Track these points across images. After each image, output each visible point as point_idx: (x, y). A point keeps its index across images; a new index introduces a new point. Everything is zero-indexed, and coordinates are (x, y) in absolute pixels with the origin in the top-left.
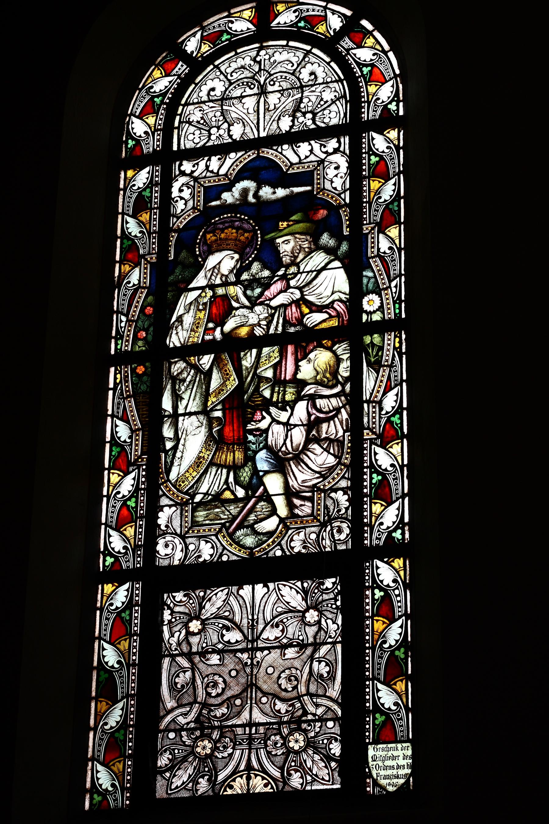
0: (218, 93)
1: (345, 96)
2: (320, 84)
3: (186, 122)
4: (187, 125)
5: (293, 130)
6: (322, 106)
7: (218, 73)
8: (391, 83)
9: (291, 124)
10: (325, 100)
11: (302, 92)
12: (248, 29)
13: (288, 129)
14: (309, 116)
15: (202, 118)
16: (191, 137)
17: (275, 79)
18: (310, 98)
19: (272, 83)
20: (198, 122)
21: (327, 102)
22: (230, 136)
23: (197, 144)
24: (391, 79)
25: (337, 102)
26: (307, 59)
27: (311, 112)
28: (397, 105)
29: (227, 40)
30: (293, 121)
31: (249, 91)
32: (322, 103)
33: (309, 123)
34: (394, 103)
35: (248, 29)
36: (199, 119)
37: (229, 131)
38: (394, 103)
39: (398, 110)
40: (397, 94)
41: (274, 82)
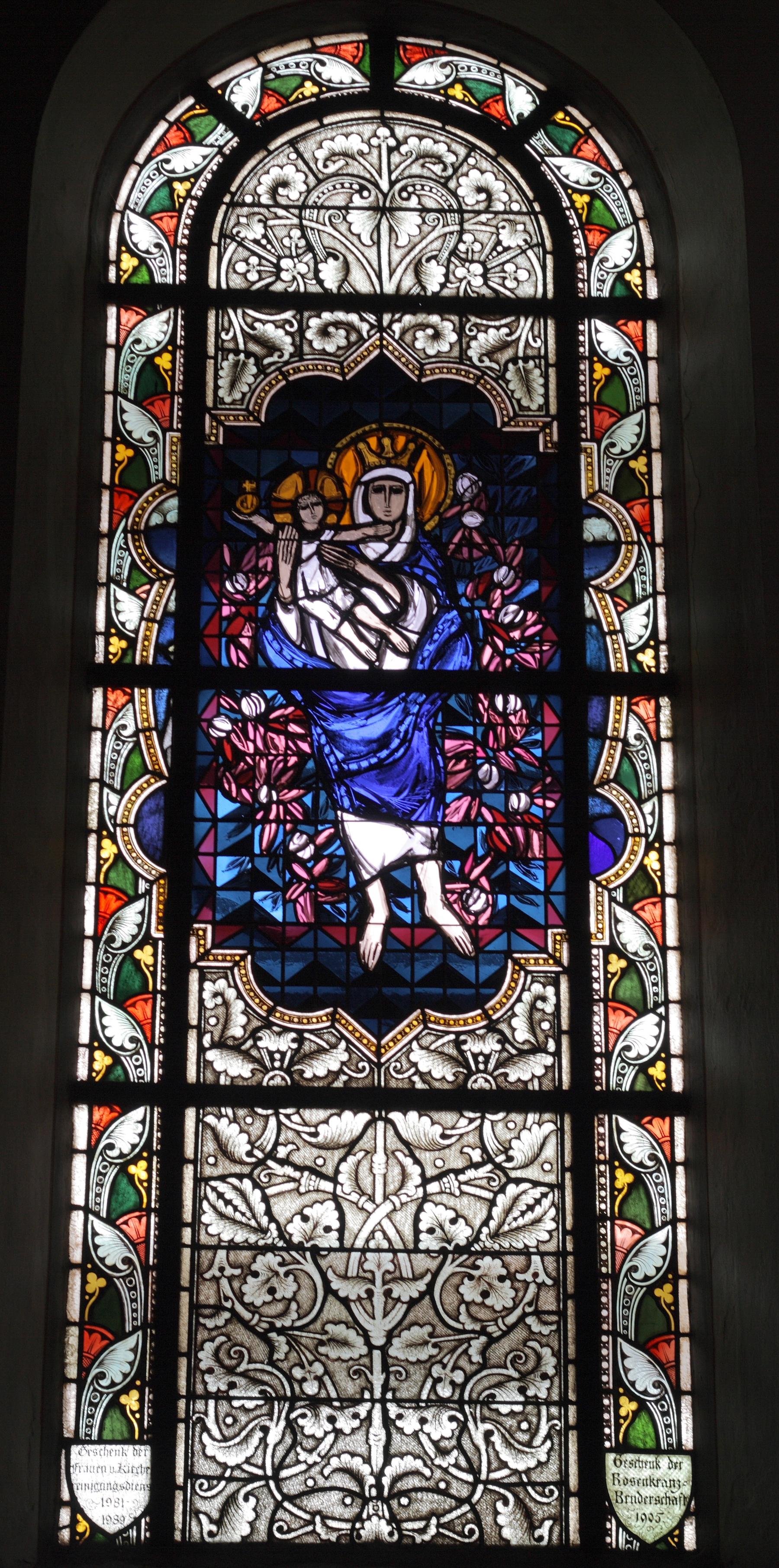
0: (294, 194)
1: (542, 245)
2: (496, 213)
3: (233, 239)
4: (233, 245)
5: (446, 292)
6: (499, 254)
7: (293, 156)
8: (628, 233)
9: (442, 280)
10: (505, 244)
11: (461, 223)
12: (354, 82)
13: (436, 288)
14: (477, 269)
15: (265, 236)
16: (241, 267)
17: (410, 189)
18: (477, 236)
19: (404, 195)
20: (257, 242)
21: (507, 249)
22: (320, 282)
23: (254, 283)
24: (627, 226)
25: (530, 253)
26: (471, 161)
27: (483, 264)
28: (643, 277)
29: (313, 95)
30: (446, 276)
31: (357, 201)
32: (500, 249)
33: (478, 282)
34: (636, 273)
35: (354, 82)
36: (259, 237)
37: (317, 271)
38: (636, 273)
39: (644, 285)
40: (640, 256)
41: (410, 194)
